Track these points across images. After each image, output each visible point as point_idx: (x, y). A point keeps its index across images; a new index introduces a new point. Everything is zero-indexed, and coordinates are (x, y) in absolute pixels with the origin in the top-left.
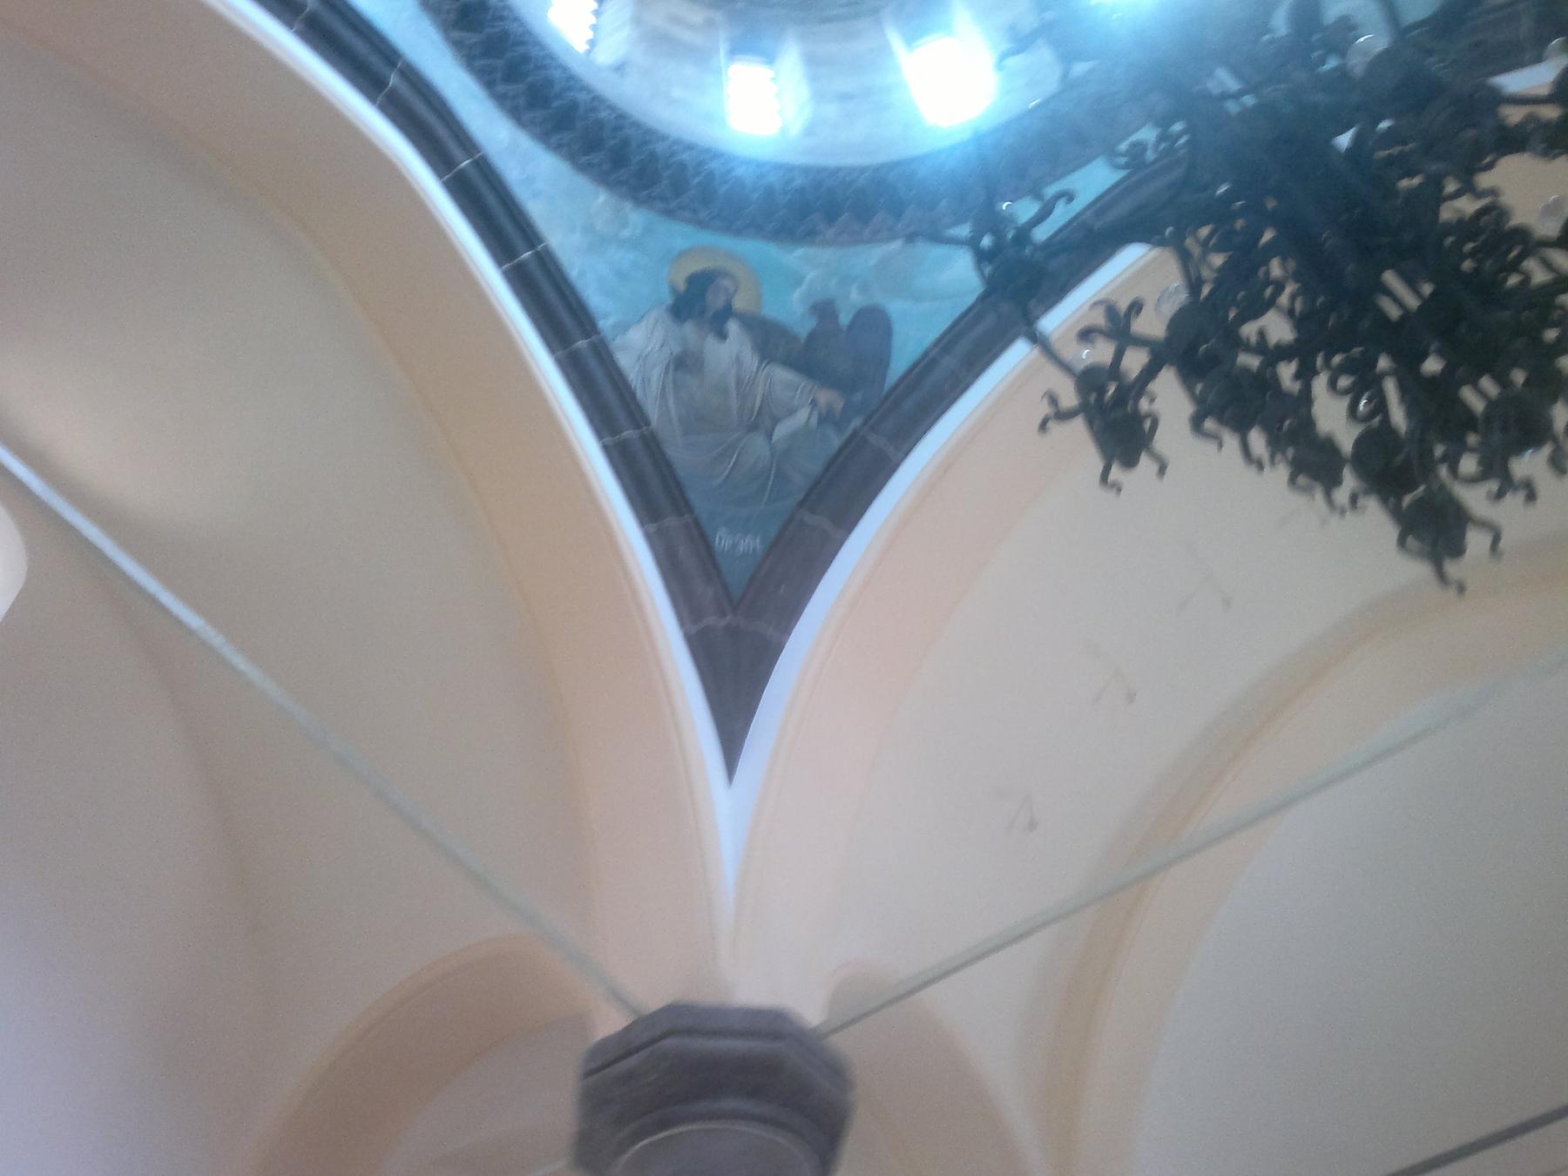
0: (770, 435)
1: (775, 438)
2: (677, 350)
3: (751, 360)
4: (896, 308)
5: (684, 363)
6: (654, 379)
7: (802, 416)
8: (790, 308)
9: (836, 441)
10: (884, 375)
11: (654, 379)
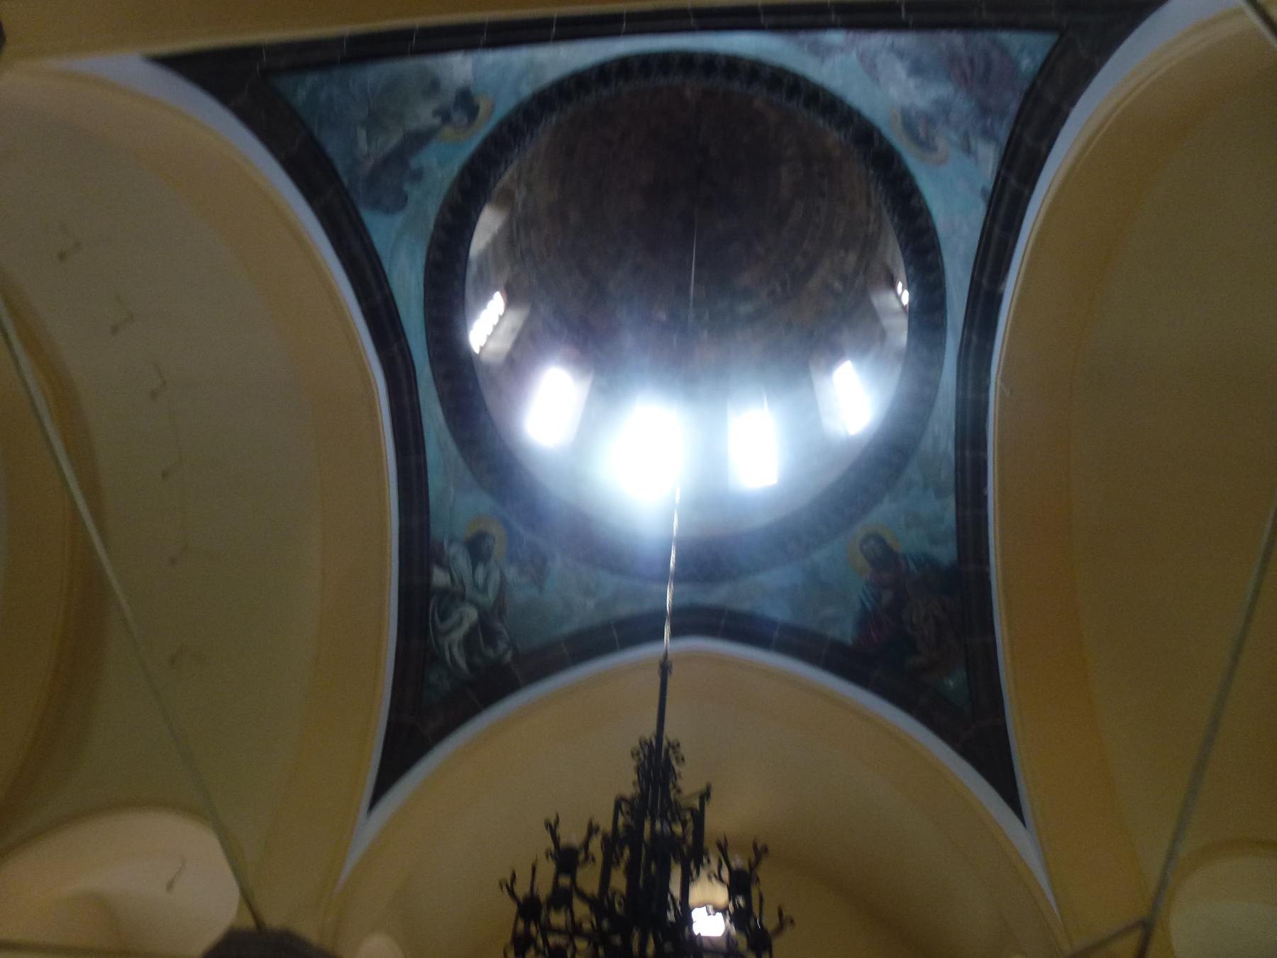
3: (413, 125)
4: (399, 219)
5: (434, 86)
9: (340, 168)
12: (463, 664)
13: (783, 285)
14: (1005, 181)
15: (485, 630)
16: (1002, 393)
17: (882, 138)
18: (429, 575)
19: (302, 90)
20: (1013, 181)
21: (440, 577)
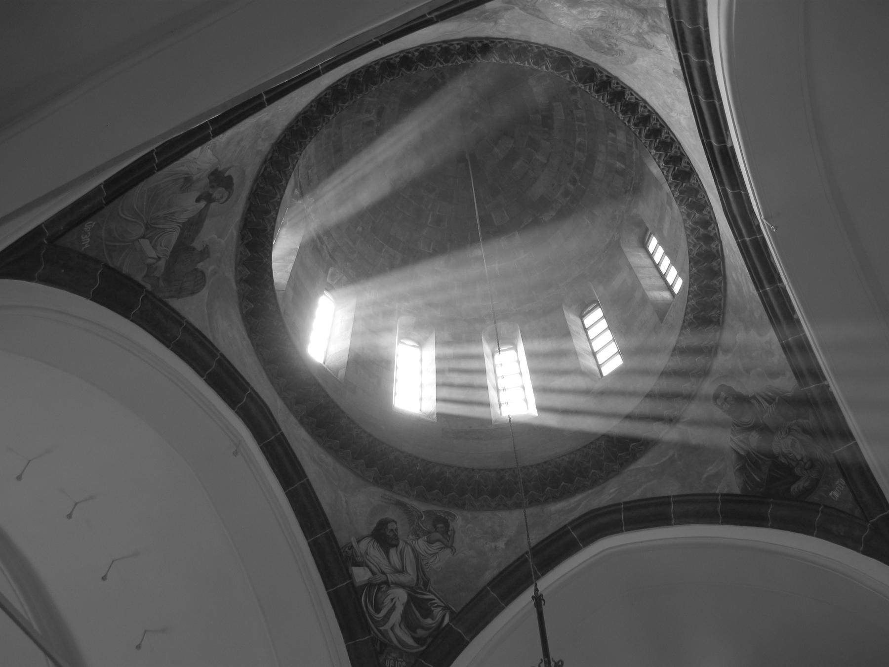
0: (143, 237)
1: (141, 241)
2: (195, 178)
3: (183, 218)
4: (204, 293)
5: (188, 181)
6: (182, 168)
7: (153, 254)
8: (207, 235)
9: (139, 278)
10: (172, 297)
11: (182, 168)
12: (410, 641)
13: (574, 182)
14: (687, 59)
15: (417, 604)
16: (771, 231)
17: (576, 58)
18: (350, 576)
19: (85, 238)
20: (694, 59)
21: (361, 575)
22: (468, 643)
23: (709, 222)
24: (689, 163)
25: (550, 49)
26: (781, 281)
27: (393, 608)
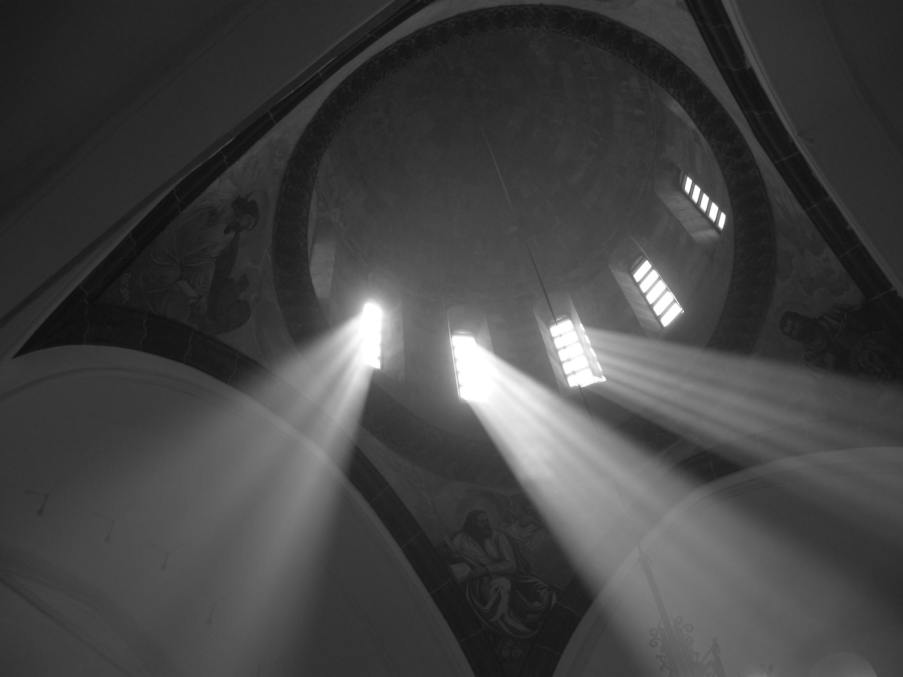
12: (522, 628)
17: (575, 11)
21: (460, 571)
22: (579, 620)
23: (742, 149)
24: (710, 94)
25: (546, 7)
26: (826, 194)
27: (499, 599)
